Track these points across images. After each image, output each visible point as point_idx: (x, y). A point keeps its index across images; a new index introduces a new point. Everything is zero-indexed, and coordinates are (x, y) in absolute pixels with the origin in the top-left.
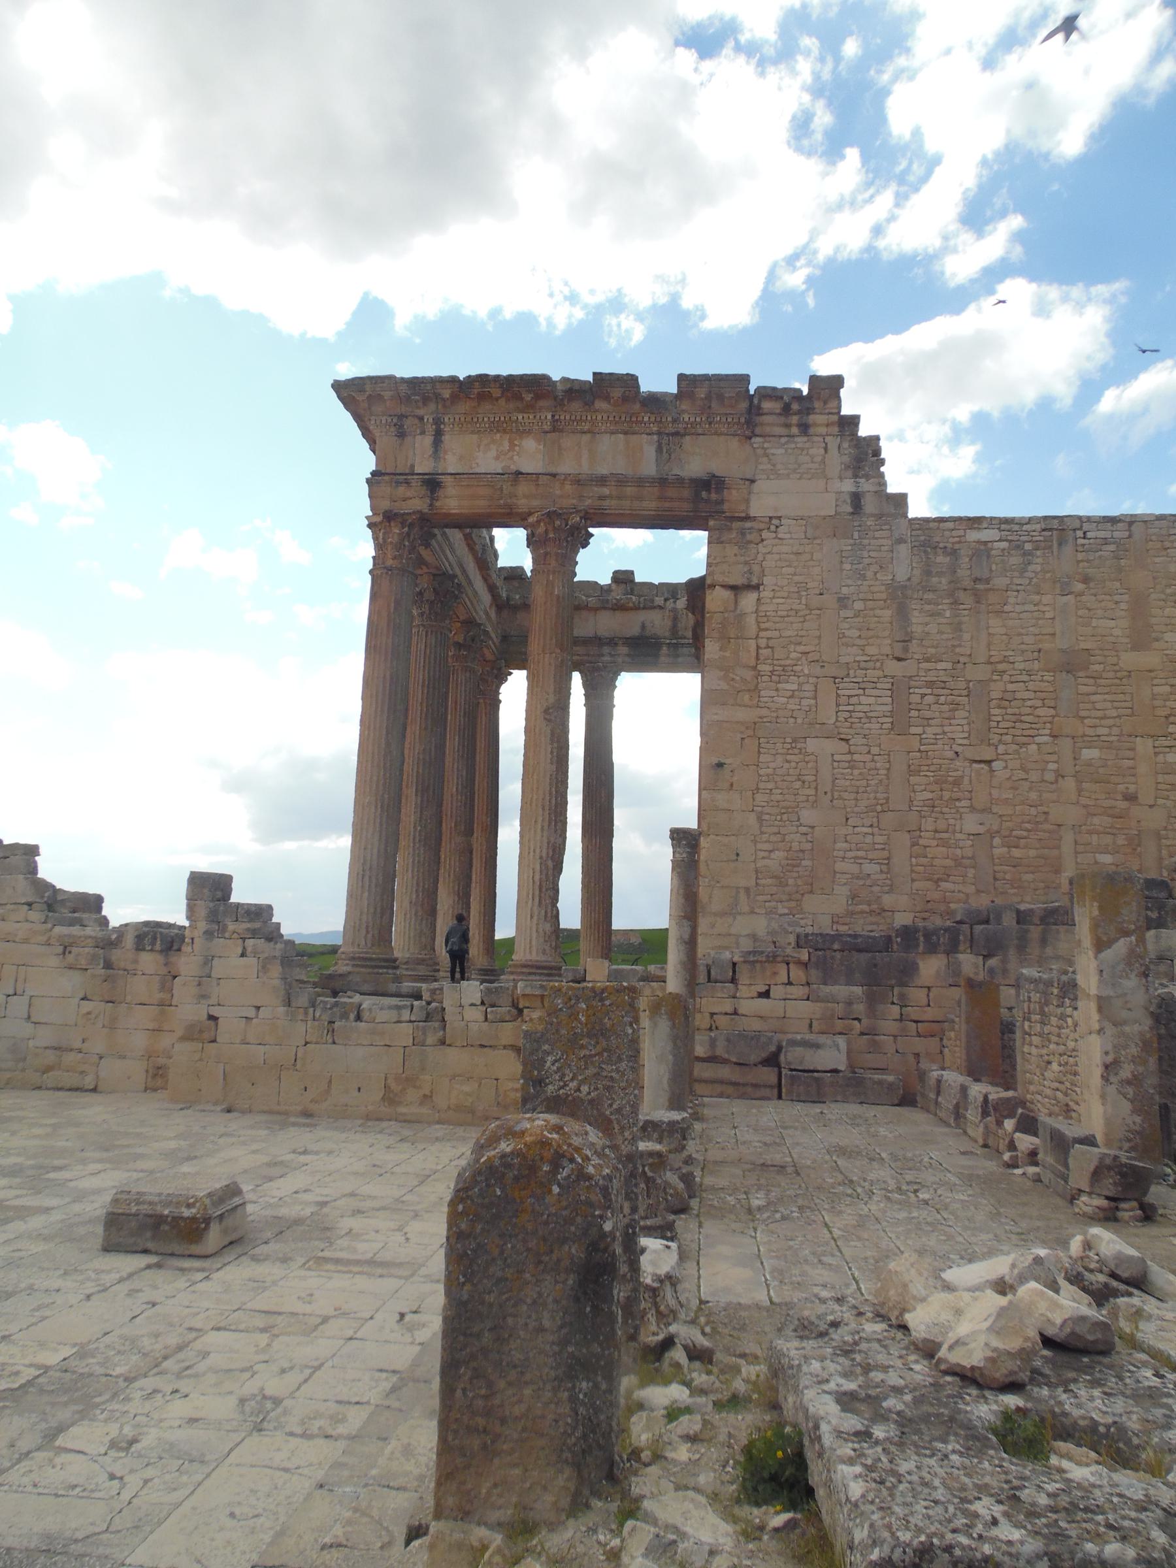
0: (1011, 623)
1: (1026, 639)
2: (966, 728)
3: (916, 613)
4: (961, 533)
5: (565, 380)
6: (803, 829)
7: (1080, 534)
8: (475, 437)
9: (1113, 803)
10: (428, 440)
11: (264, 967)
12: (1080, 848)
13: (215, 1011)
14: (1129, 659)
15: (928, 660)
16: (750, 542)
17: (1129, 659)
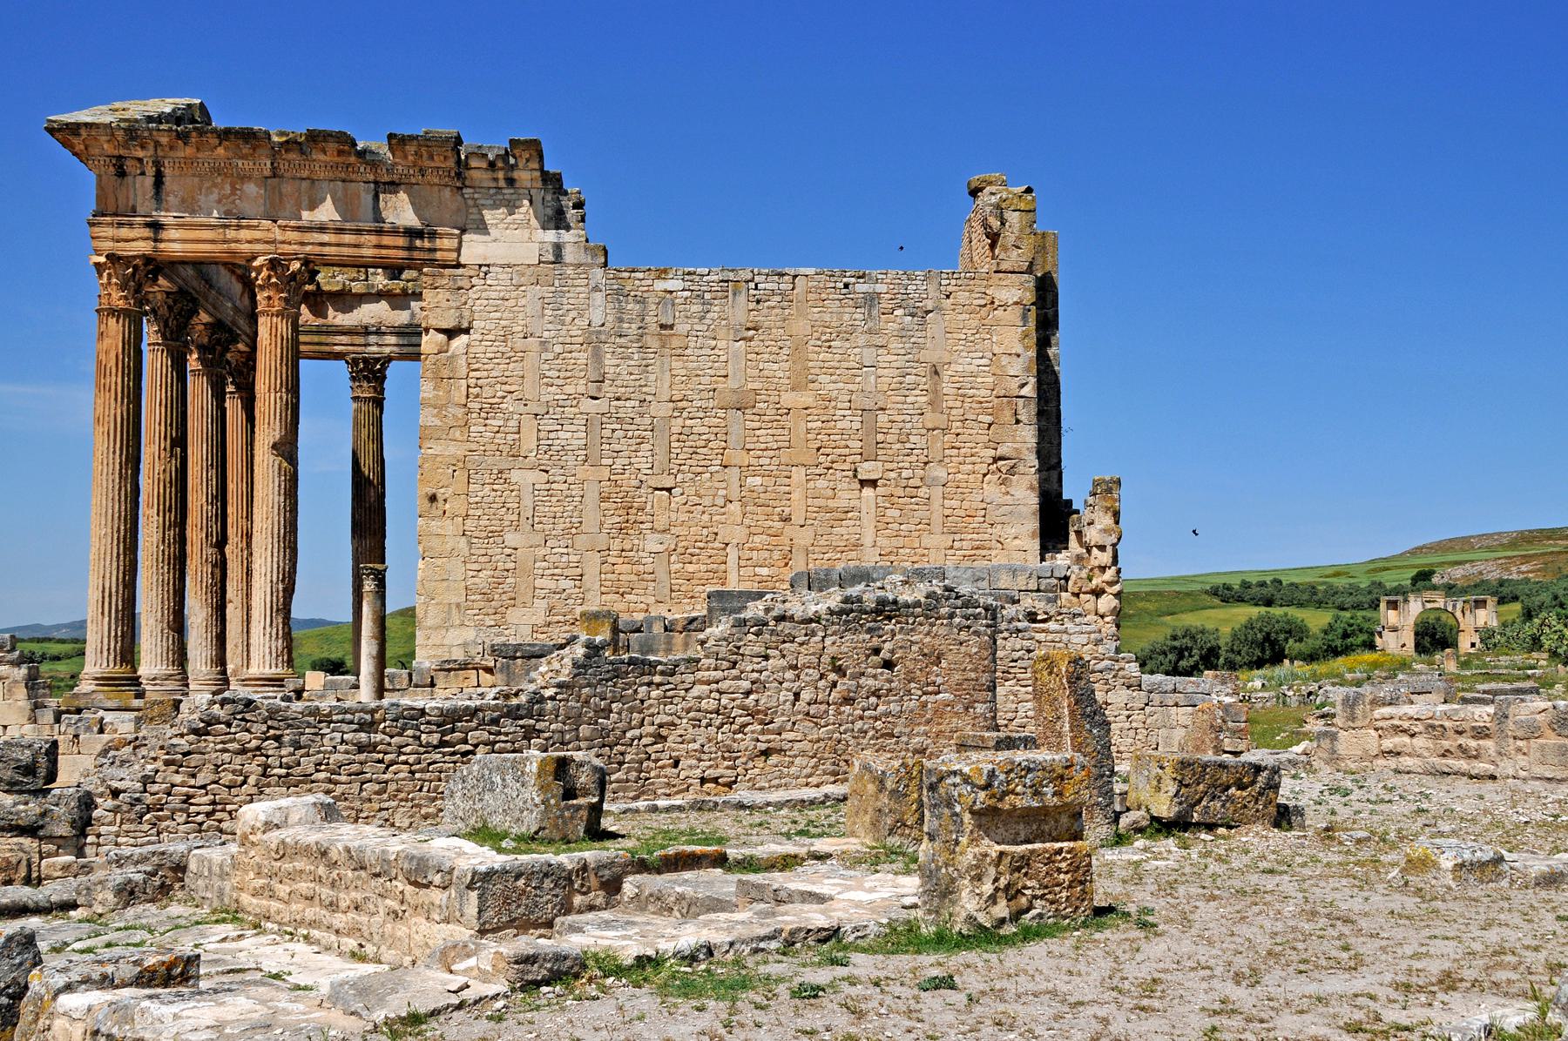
0: (691, 365)
1: (703, 380)
2: (650, 460)
3: (608, 356)
4: (650, 282)
6: (508, 551)
7: (752, 285)
8: (196, 180)
9: (771, 523)
10: (149, 181)
12: (743, 563)
14: (788, 399)
15: (618, 399)
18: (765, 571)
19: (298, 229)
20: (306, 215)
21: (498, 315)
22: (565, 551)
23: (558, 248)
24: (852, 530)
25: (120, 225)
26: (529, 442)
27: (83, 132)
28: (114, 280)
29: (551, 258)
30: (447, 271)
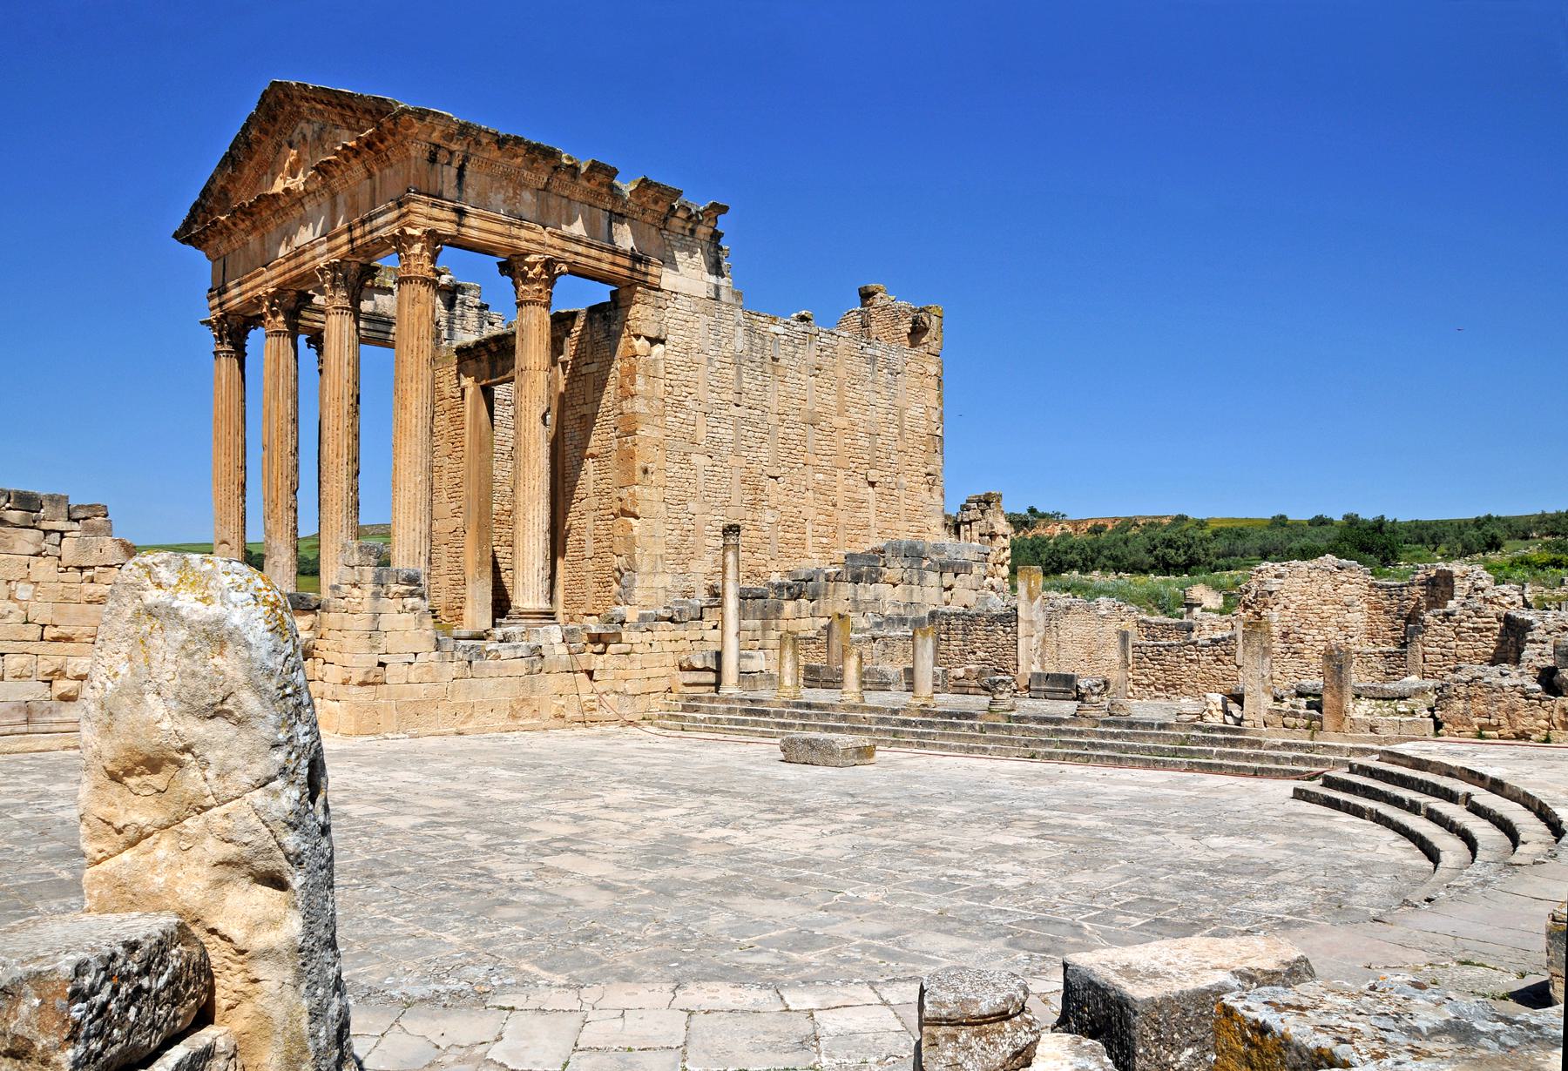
3: (745, 375)
4: (766, 325)
6: (690, 516)
8: (489, 178)
10: (454, 172)
11: (420, 621)
13: (384, 659)
14: (837, 421)
16: (660, 307)
18: (824, 540)
19: (562, 237)
20: (564, 227)
21: (682, 333)
22: (721, 518)
23: (717, 288)
24: (865, 515)
25: (434, 205)
27: (428, 119)
29: (713, 296)
30: (652, 292)
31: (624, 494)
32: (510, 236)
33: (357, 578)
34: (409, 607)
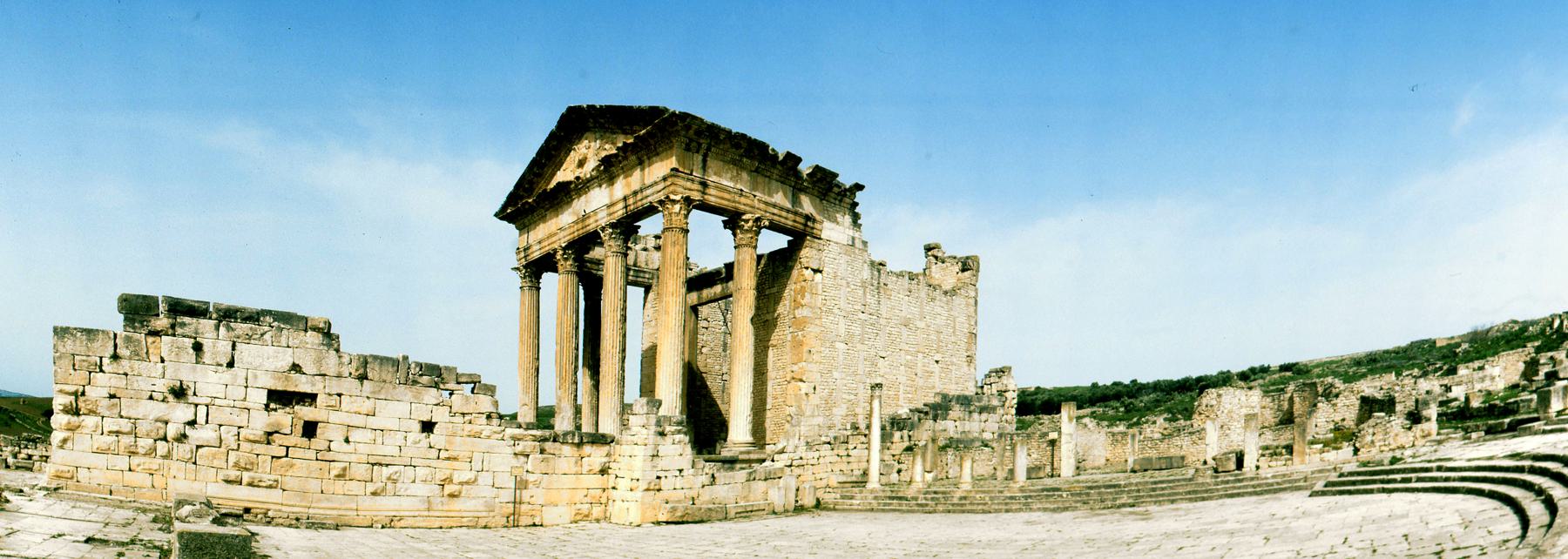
5: (773, 150)
10: (700, 158)
14: (921, 325)
17: (921, 325)
23: (853, 239)
26: (842, 330)
28: (683, 212)
29: (851, 243)
31: (795, 368)
32: (734, 202)
33: (646, 422)
34: (677, 441)
